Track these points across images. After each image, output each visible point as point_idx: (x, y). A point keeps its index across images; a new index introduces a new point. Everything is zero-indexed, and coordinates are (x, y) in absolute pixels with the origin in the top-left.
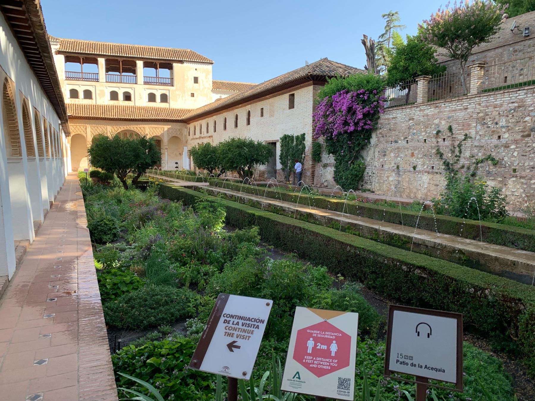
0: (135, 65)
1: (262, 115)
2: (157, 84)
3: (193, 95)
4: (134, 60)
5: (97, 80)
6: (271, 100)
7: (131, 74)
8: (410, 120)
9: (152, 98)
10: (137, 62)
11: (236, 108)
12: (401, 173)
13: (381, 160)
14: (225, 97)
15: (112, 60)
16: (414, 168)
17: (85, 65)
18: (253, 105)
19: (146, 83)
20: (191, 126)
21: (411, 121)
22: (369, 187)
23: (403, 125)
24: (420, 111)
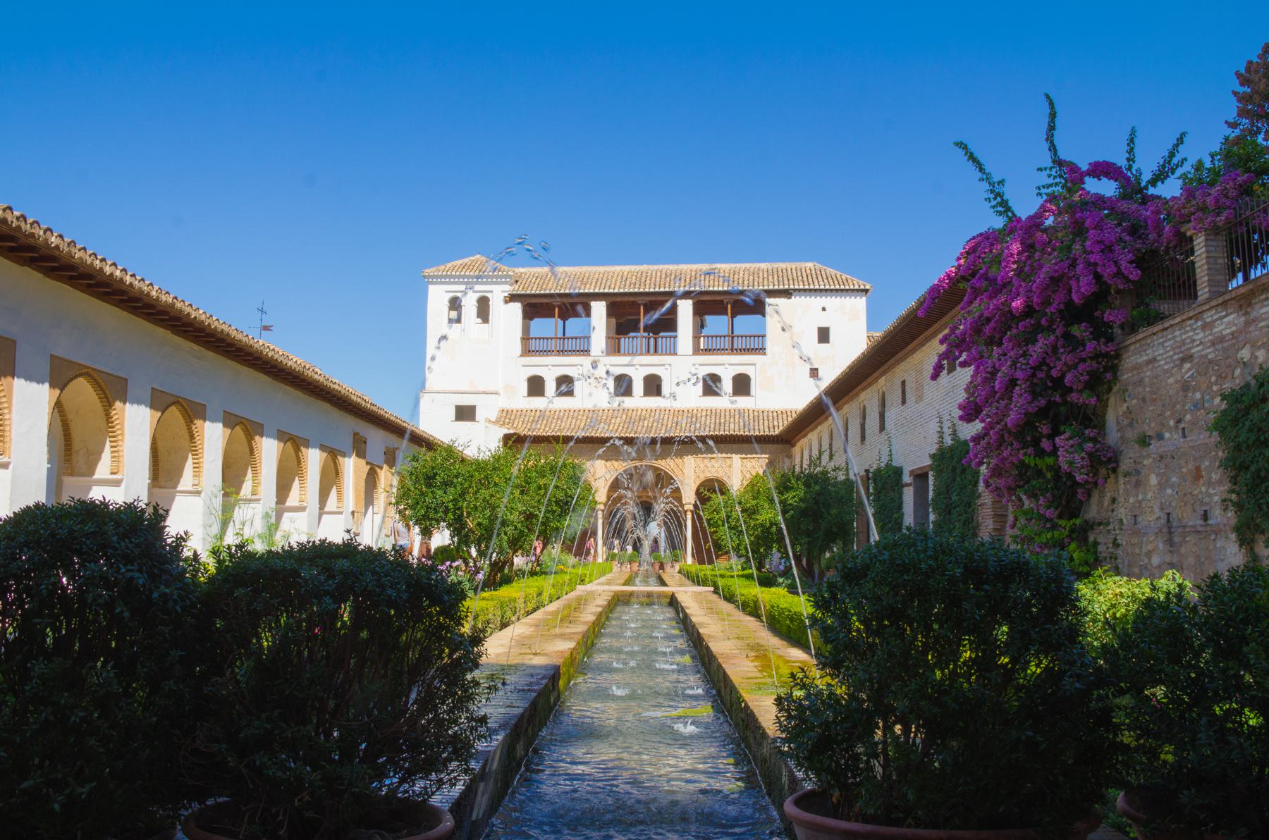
0: (673, 310)
1: (904, 402)
2: (733, 350)
5: (586, 352)
8: (1183, 360)
11: (863, 389)
12: (1176, 539)
13: (1132, 500)
15: (623, 304)
16: (1205, 517)
17: (571, 322)
19: (697, 351)
20: (796, 450)
21: (1187, 366)
23: (1171, 381)
24: (1205, 327)
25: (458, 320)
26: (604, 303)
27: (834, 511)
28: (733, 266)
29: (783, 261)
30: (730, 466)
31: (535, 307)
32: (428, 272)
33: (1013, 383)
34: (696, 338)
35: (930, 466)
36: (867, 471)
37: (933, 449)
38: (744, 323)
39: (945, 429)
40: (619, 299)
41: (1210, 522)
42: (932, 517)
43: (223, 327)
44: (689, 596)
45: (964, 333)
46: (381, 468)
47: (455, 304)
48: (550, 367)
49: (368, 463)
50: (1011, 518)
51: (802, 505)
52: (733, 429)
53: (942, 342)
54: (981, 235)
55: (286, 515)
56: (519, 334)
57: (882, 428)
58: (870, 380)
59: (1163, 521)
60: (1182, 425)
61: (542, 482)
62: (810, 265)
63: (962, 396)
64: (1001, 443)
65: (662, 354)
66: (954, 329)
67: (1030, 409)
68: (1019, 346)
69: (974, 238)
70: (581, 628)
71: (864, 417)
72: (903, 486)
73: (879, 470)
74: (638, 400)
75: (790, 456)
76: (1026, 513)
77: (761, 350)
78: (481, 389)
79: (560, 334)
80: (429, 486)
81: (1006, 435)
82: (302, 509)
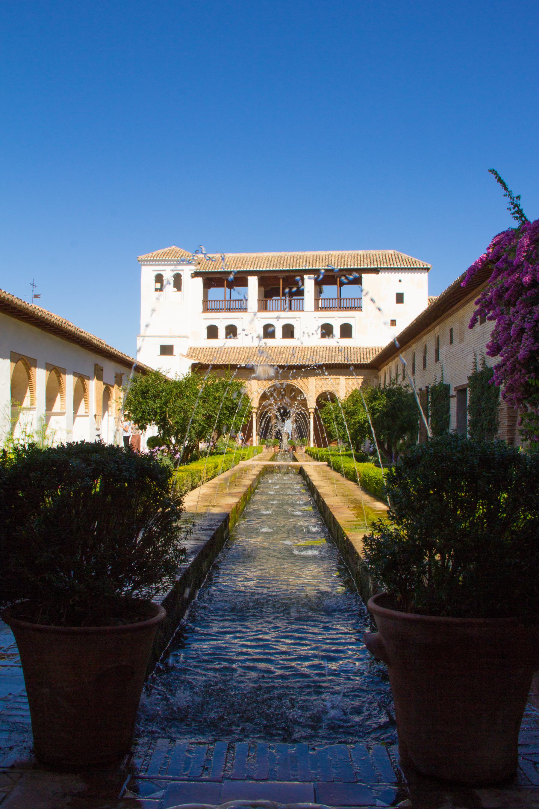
1: (451, 342)
2: (341, 308)
3: (393, 323)
5: (245, 310)
9: (327, 330)
11: (425, 334)
15: (269, 278)
19: (317, 308)
20: (381, 373)
25: (161, 290)
27: (405, 414)
28: (341, 252)
29: (374, 249)
30: (339, 384)
31: (212, 280)
32: (141, 257)
33: (522, 331)
34: (317, 300)
35: (468, 384)
36: (427, 387)
37: (470, 373)
38: (348, 291)
39: (478, 361)
40: (266, 275)
42: (468, 417)
43: (9, 297)
44: (312, 468)
45: (491, 298)
46: (113, 387)
47: (159, 278)
48: (221, 320)
49: (104, 384)
50: (519, 418)
51: (385, 410)
52: (340, 359)
53: (476, 303)
54: (503, 233)
55: (53, 418)
56: (201, 297)
57: (437, 359)
58: (429, 328)
61: (217, 395)
62: (391, 252)
63: (488, 339)
64: (513, 370)
65: (294, 311)
66: (484, 295)
67: (533, 348)
68: (527, 307)
69: (499, 235)
70: (242, 489)
71: (425, 352)
72: (450, 397)
73: (435, 387)
75: (377, 377)
76: (529, 415)
78: (178, 335)
79: (228, 298)
80: (144, 398)
81: (517, 365)
82: (63, 414)
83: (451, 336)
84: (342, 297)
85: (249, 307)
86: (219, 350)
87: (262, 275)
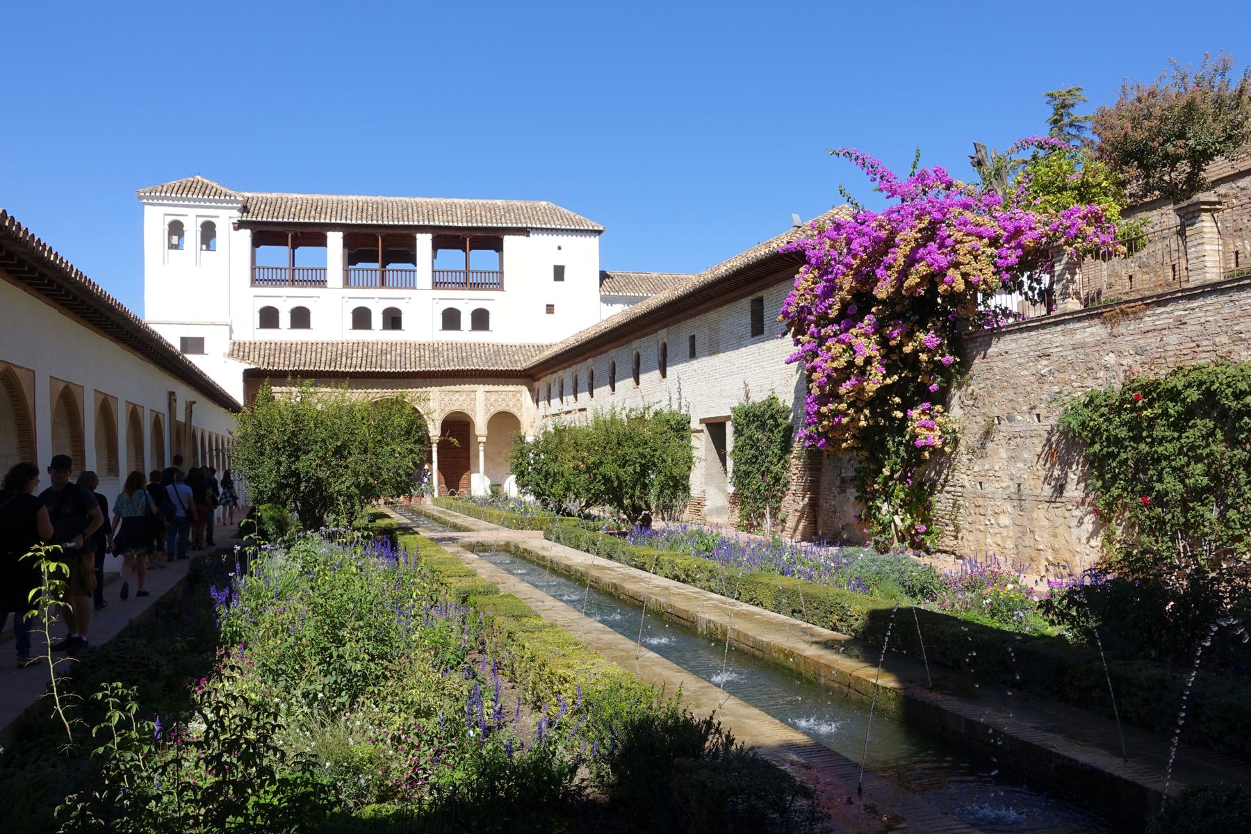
3: (550, 309)
4: (412, 231)
5: (322, 283)
6: (712, 316)
7: (409, 266)
10: (419, 236)
14: (616, 314)
17: (301, 251)
18: (673, 329)
19: (436, 285)
22: (949, 542)
23: (1025, 372)
24: (1064, 333)
26: (341, 234)
28: (467, 201)
29: (518, 199)
31: (265, 234)
38: (481, 259)
40: (357, 231)
41: (1065, 494)
47: (176, 228)
48: (285, 299)
59: (1013, 489)
60: (1036, 412)
62: (544, 203)
74: (377, 333)
77: (499, 286)
83: (693, 346)
84: (471, 269)
85: (328, 279)
86: (279, 348)
87: (351, 230)
